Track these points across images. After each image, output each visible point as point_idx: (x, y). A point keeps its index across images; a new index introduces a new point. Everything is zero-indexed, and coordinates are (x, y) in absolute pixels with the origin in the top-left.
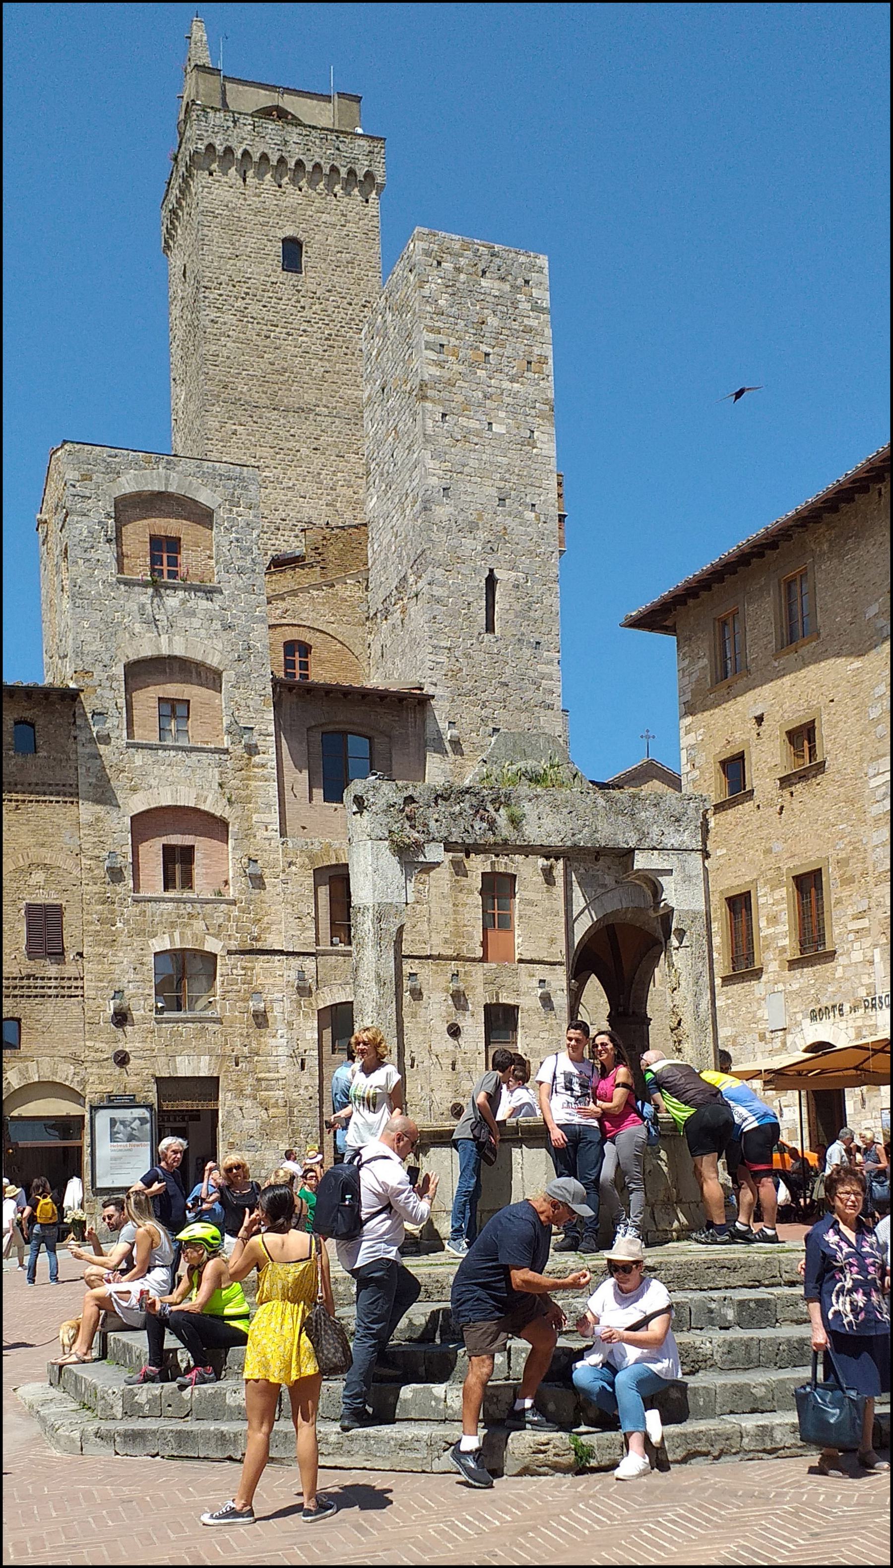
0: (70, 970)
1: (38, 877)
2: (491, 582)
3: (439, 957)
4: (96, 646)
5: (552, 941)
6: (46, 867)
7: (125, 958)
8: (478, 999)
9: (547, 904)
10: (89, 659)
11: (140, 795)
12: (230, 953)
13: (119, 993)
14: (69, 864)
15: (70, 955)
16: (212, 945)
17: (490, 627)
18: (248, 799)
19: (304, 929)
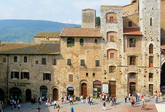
0: (100, 68)
1: (97, 57)
2: (151, 19)
3: (143, 67)
4: (104, 31)
5: (158, 65)
6: (98, 56)
7: (106, 66)
8: (148, 72)
9: (158, 60)
10: (103, 32)
11: (108, 48)
12: (118, 66)
13: (105, 71)
14: (100, 56)
15: (100, 66)
16: (116, 65)
17: (151, 25)
18: (120, 48)
19: (126, 63)
